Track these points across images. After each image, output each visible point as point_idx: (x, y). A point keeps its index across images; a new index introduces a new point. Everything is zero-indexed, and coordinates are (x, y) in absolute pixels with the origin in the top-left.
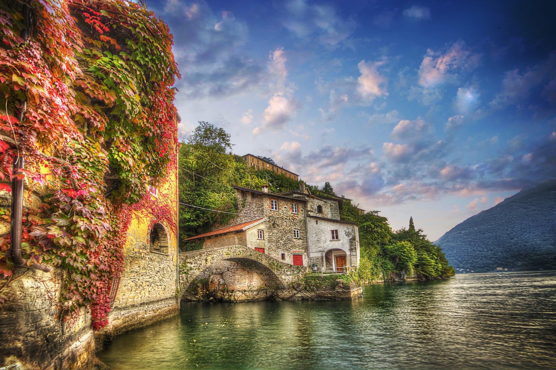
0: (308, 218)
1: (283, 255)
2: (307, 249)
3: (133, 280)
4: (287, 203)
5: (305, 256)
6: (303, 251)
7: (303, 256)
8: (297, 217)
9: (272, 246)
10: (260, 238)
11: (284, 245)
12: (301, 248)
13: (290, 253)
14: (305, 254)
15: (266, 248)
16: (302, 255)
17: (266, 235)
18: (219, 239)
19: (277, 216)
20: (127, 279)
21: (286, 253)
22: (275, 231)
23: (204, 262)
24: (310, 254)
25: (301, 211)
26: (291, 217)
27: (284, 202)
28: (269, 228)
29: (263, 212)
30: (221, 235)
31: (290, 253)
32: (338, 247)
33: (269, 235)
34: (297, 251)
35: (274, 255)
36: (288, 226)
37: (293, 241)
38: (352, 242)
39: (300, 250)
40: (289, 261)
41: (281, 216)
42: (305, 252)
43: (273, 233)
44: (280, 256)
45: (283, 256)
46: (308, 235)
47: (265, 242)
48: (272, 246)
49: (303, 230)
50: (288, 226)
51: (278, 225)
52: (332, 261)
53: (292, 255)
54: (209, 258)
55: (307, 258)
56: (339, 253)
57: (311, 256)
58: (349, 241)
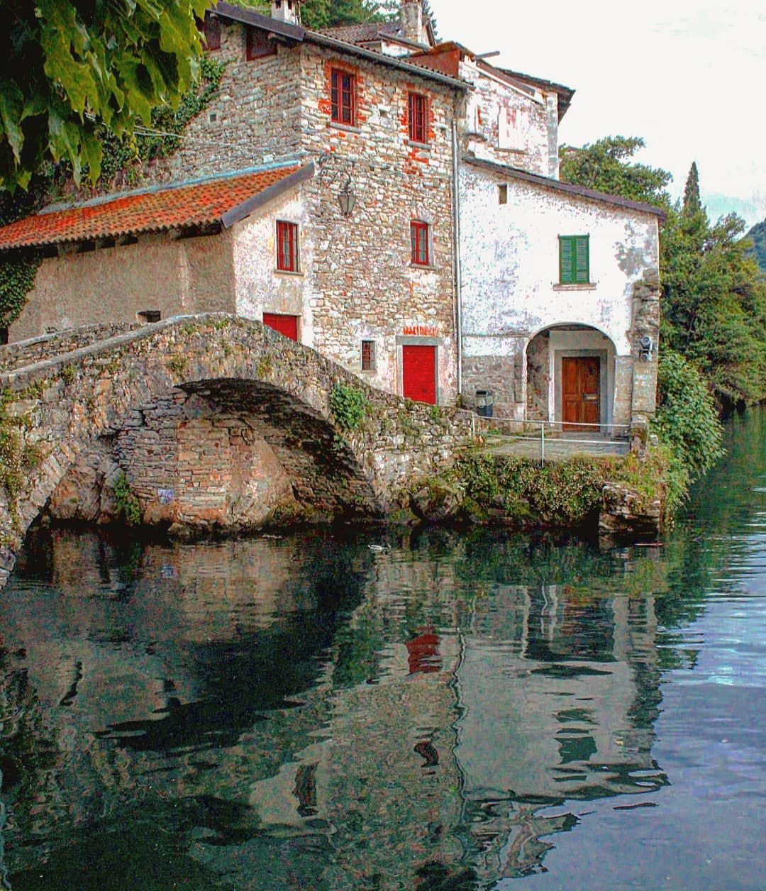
0: (463, 170)
1: (367, 346)
2: (452, 316)
4: (389, 89)
6: (441, 325)
7: (440, 349)
8: (425, 161)
9: (327, 303)
11: (375, 297)
12: (432, 311)
15: (307, 317)
17: (307, 247)
18: (100, 262)
23: (79, 408)
25: (438, 134)
27: (379, 87)
28: (320, 214)
30: (109, 242)
31: (392, 340)
32: (587, 321)
35: (336, 349)
37: (406, 282)
38: (644, 301)
39: (430, 321)
42: (446, 333)
43: (334, 240)
44: (356, 354)
46: (463, 252)
47: (302, 287)
48: (327, 303)
52: (546, 379)
54: (102, 386)
55: (452, 358)
56: (575, 345)
57: (469, 352)
58: (630, 293)
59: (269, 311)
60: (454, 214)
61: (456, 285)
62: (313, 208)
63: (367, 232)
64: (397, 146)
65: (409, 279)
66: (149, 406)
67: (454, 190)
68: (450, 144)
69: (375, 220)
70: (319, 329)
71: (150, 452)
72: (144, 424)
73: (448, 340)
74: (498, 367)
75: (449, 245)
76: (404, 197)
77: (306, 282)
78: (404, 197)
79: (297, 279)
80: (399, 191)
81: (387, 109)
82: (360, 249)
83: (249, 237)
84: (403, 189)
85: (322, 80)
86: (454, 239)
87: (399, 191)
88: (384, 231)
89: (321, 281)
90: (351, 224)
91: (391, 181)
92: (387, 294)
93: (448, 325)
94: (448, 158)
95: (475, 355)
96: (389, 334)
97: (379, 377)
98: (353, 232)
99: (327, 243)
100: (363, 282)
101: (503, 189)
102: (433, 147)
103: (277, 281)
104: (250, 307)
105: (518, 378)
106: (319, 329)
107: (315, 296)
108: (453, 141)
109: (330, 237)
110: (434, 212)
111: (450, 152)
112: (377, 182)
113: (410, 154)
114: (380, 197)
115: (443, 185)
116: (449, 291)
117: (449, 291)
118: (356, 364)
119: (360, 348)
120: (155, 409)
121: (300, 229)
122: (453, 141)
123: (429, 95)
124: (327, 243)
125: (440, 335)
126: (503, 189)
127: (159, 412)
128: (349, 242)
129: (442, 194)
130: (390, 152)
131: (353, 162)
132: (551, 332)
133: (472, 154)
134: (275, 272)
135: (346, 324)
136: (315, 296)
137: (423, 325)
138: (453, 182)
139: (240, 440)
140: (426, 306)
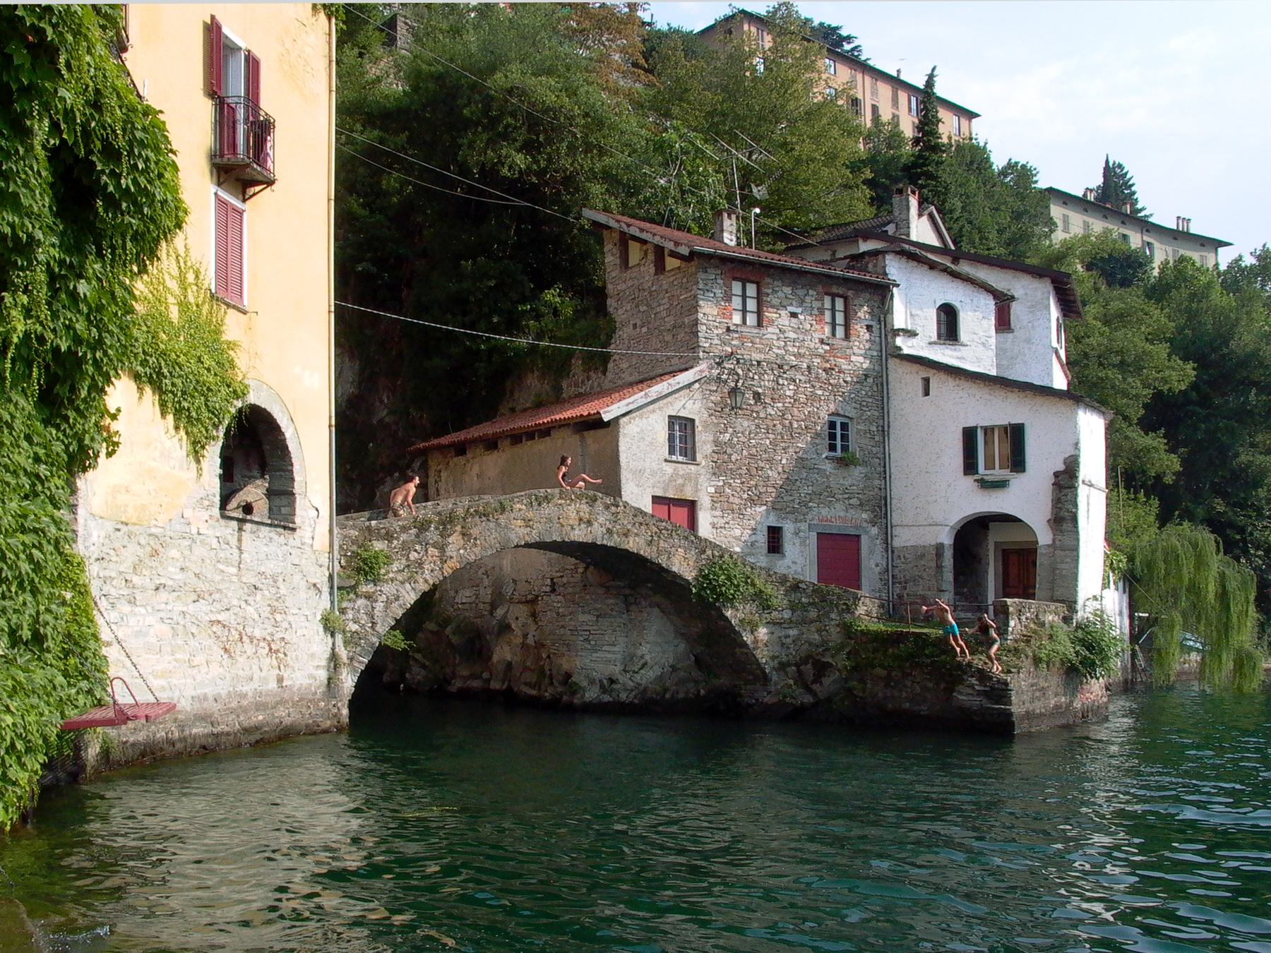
2: (881, 508)
3: (162, 615)
4: (801, 292)
5: (873, 539)
6: (865, 516)
7: (865, 541)
8: (847, 358)
10: (674, 458)
12: (854, 501)
13: (804, 526)
14: (874, 531)
15: (704, 501)
16: (858, 537)
17: (704, 442)
19: (756, 356)
20: (142, 610)
21: (788, 528)
22: (744, 424)
24: (896, 531)
26: (817, 361)
29: (696, 334)
31: (804, 526)
33: (716, 442)
34: (838, 516)
36: (802, 398)
39: (852, 511)
40: (800, 561)
41: (772, 356)
45: (775, 540)
49: (870, 421)
50: (802, 398)
51: (757, 396)
53: (814, 535)
55: (879, 548)
59: (660, 493)
60: (883, 408)
61: (884, 475)
62: (711, 405)
63: (774, 426)
64: (812, 346)
65: (825, 470)
66: (558, 574)
67: (882, 384)
68: (877, 339)
69: (783, 415)
70: (718, 513)
71: (558, 614)
72: (553, 591)
73: (874, 531)
74: (923, 556)
75: (877, 438)
76: (820, 392)
77: (703, 471)
78: (820, 392)
79: (692, 467)
80: (813, 387)
81: (799, 310)
82: (768, 442)
83: (638, 430)
84: (817, 385)
85: (721, 288)
86: (884, 431)
87: (813, 387)
88: (795, 425)
89: (718, 469)
90: (755, 418)
91: (802, 378)
92: (798, 483)
93: (875, 516)
94: (875, 354)
95: (903, 545)
96: (801, 521)
97: (787, 561)
98: (758, 426)
99: (727, 436)
100: (769, 472)
101: (927, 381)
102: (857, 343)
103: (669, 468)
104: (636, 490)
105: (939, 567)
106: (718, 513)
107: (713, 483)
108: (880, 337)
109: (730, 430)
110: (858, 406)
111: (878, 348)
112: (786, 379)
113: (826, 352)
114: (788, 393)
115: (870, 380)
116: (877, 482)
117: (877, 482)
118: (761, 547)
119: (766, 533)
120: (562, 577)
121: (697, 423)
122: (880, 337)
123: (850, 293)
124: (727, 436)
125: (865, 525)
126: (927, 381)
127: (565, 580)
128: (752, 435)
129: (868, 389)
130: (802, 351)
131: (759, 363)
132: (991, 525)
133: (900, 349)
134: (666, 461)
135: (749, 510)
136: (713, 483)
137: (842, 514)
138: (882, 376)
139: (633, 607)
140: (846, 496)
